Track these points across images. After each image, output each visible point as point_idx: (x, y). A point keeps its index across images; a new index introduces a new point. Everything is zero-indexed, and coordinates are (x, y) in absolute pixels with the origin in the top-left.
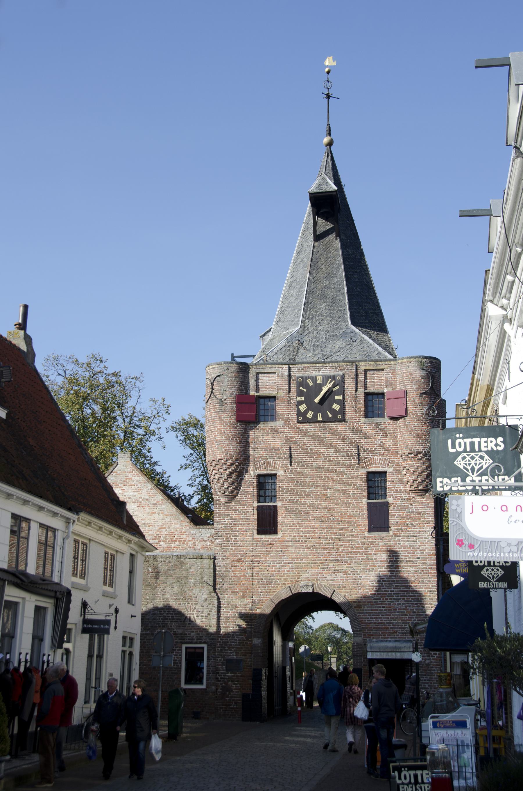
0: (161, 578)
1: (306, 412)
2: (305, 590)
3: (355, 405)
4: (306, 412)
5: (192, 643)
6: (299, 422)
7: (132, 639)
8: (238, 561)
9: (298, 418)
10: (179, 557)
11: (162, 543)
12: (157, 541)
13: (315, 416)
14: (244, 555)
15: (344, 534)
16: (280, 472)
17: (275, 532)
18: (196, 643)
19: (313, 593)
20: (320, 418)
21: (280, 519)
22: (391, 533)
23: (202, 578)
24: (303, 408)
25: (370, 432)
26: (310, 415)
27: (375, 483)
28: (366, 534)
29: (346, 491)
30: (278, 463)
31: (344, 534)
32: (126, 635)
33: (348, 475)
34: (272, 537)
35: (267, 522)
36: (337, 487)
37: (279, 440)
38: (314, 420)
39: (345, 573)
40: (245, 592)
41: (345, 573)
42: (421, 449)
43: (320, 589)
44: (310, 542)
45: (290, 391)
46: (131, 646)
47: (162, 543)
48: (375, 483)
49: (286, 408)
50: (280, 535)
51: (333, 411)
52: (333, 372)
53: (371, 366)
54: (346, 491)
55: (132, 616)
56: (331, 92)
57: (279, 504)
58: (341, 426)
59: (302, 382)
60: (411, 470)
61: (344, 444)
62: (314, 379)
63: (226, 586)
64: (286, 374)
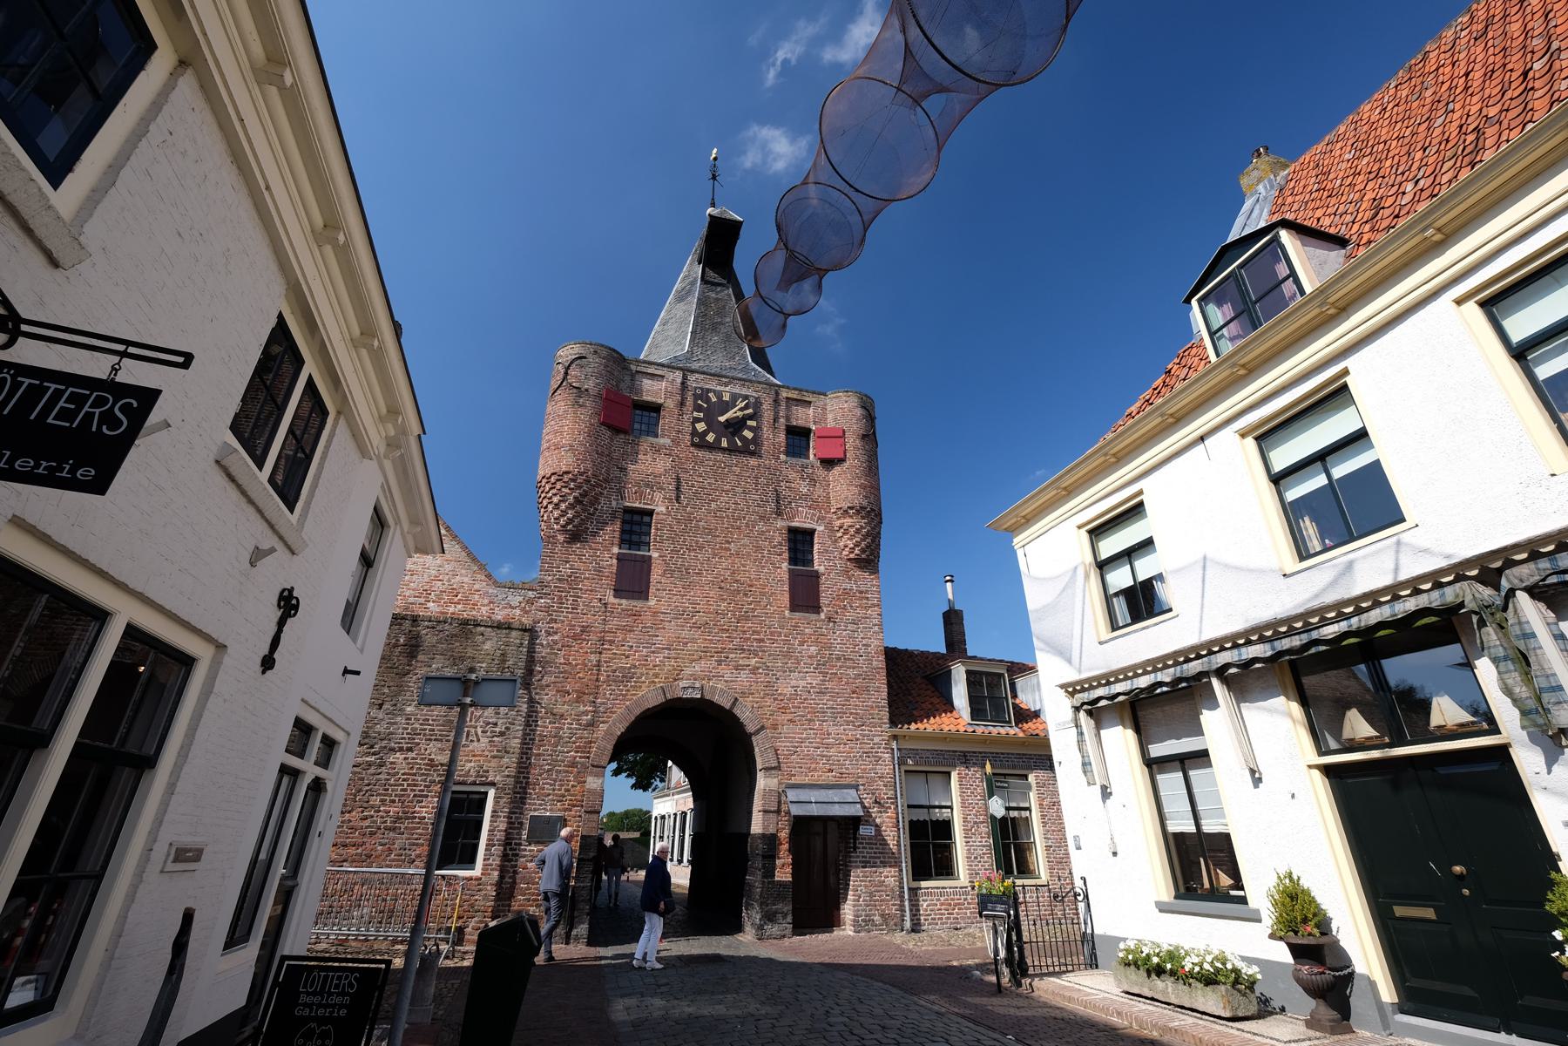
0: (420, 657)
1: (705, 433)
2: (688, 695)
3: (774, 439)
4: (705, 433)
5: (463, 783)
7: (329, 744)
8: (575, 637)
10: (465, 622)
11: (431, 605)
12: (422, 600)
13: (718, 440)
14: (584, 629)
15: (754, 610)
16: (661, 509)
18: (474, 783)
19: (702, 699)
20: (724, 444)
21: (655, 575)
22: (823, 616)
23: (504, 661)
24: (701, 427)
25: (793, 475)
26: (711, 437)
27: (800, 543)
28: (787, 613)
29: (758, 548)
30: (658, 496)
31: (754, 610)
32: (311, 718)
33: (761, 526)
34: (639, 604)
35: (633, 580)
36: (746, 541)
37: (661, 464)
39: (754, 670)
40: (581, 694)
41: (754, 670)
42: (865, 503)
43: (714, 694)
44: (700, 618)
45: (682, 404)
46: (325, 761)
47: (431, 605)
48: (800, 543)
50: (652, 602)
51: (744, 439)
52: (744, 392)
53: (794, 395)
54: (758, 548)
55: (346, 671)
57: (655, 555)
58: (753, 462)
59: (703, 394)
60: (852, 531)
62: (719, 395)
63: (547, 679)
64: (679, 380)
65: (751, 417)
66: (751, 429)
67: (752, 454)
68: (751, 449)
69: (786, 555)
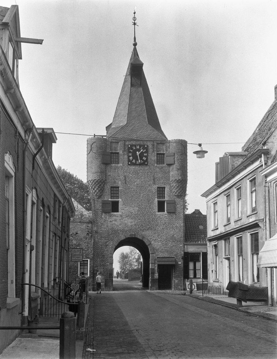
4: (132, 160)
6: (129, 164)
9: (128, 163)
17: (118, 211)
24: (131, 158)
38: (135, 164)
42: (180, 178)
49: (124, 157)
56: (136, 22)
57: (120, 200)
60: (176, 187)
61: (148, 175)
65: (145, 152)
66: (145, 156)
67: (147, 165)
68: (144, 163)
69: (156, 196)
